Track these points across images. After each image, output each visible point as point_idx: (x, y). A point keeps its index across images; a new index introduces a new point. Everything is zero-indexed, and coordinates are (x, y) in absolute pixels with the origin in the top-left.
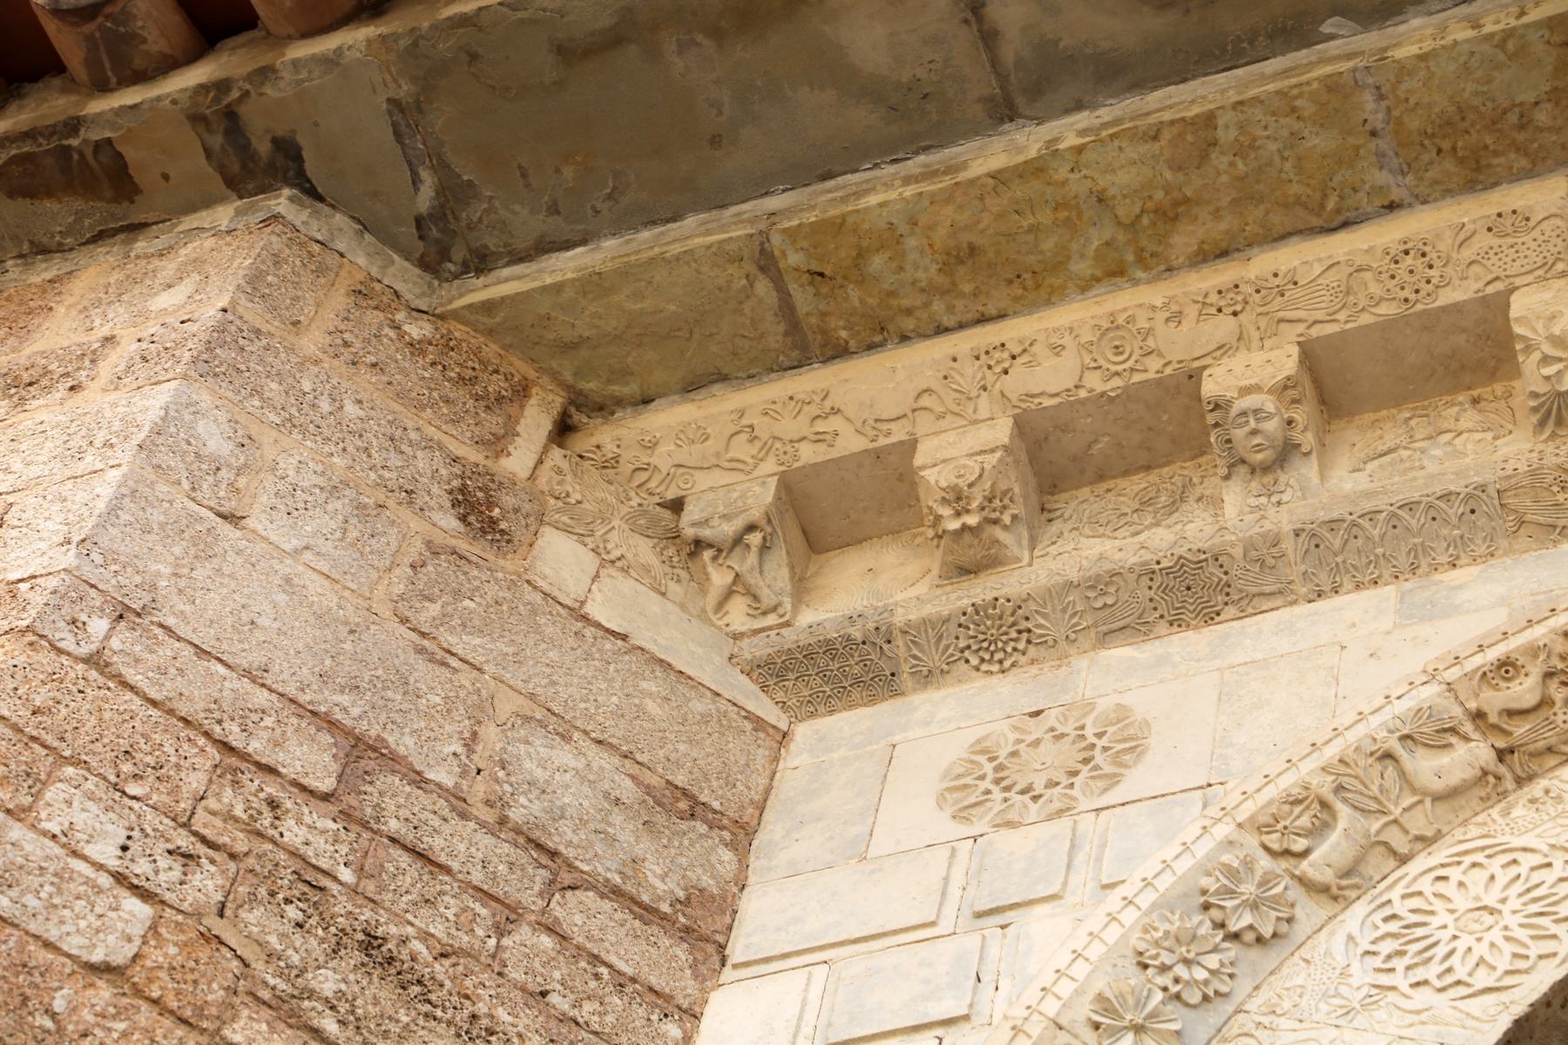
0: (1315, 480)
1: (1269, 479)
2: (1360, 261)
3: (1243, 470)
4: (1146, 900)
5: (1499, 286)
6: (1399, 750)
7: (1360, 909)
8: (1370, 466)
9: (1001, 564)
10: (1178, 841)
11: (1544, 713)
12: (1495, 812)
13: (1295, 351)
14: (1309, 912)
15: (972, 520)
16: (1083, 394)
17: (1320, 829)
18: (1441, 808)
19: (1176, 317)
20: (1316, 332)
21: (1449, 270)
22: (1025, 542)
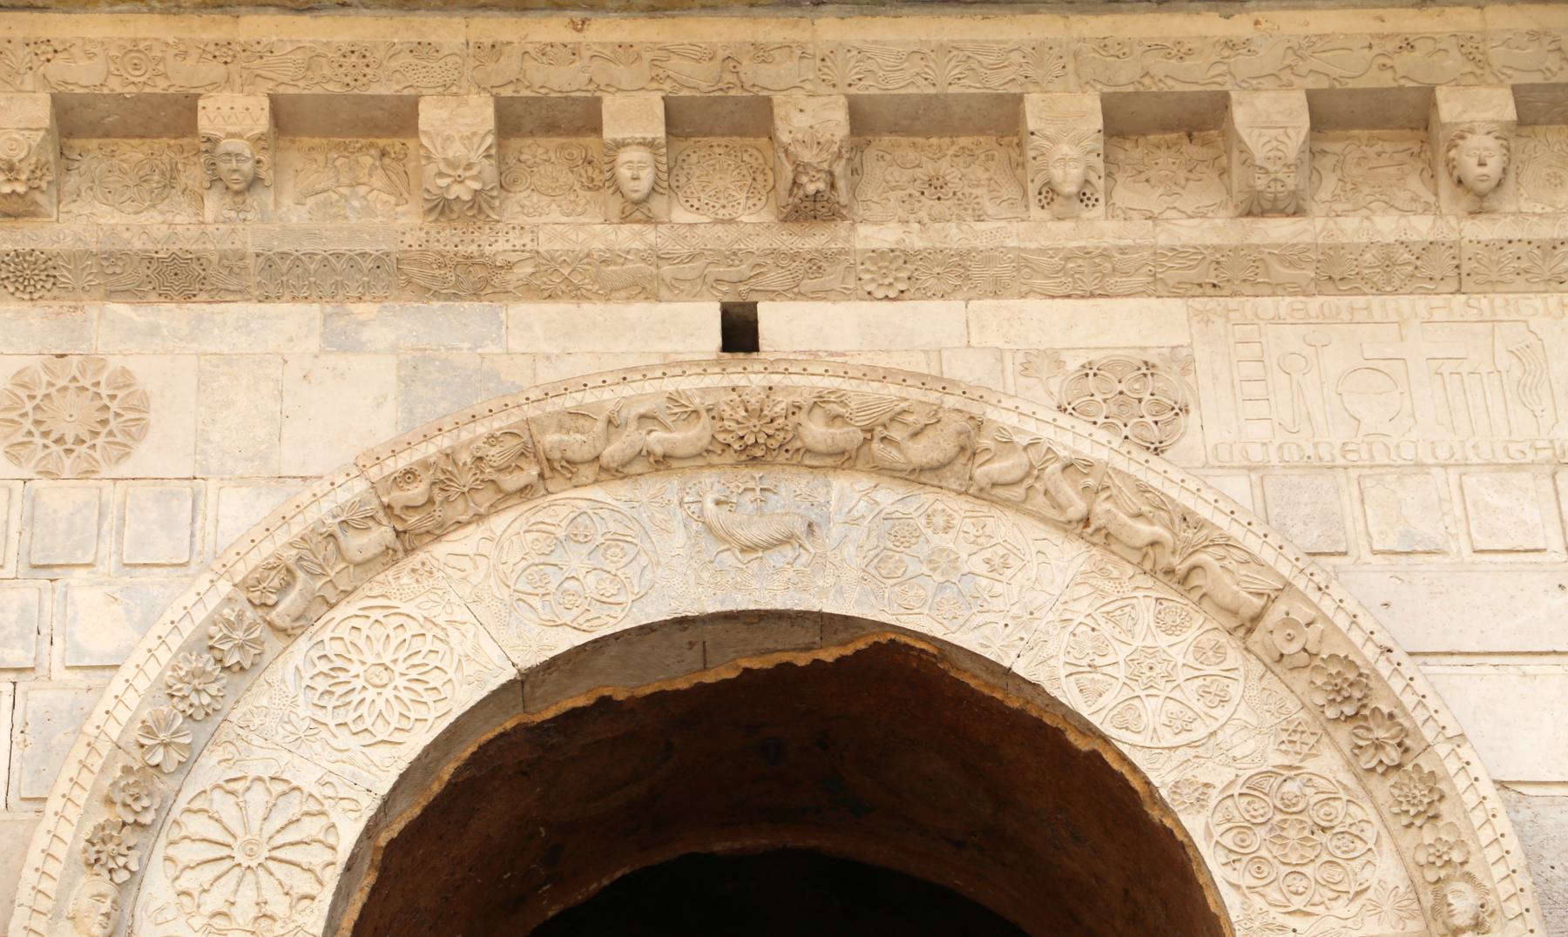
0: (271, 207)
1: (239, 199)
2: (320, 50)
3: (220, 185)
4: (175, 642)
5: (412, 92)
6: (339, 534)
7: (302, 644)
8: (310, 201)
9: (34, 214)
10: (194, 590)
11: (428, 509)
12: (391, 573)
13: (266, 103)
14: (273, 644)
15: (21, 188)
16: (106, 91)
17: (286, 587)
18: (359, 570)
19: (184, 55)
20: (281, 90)
21: (380, 72)
22: (55, 200)
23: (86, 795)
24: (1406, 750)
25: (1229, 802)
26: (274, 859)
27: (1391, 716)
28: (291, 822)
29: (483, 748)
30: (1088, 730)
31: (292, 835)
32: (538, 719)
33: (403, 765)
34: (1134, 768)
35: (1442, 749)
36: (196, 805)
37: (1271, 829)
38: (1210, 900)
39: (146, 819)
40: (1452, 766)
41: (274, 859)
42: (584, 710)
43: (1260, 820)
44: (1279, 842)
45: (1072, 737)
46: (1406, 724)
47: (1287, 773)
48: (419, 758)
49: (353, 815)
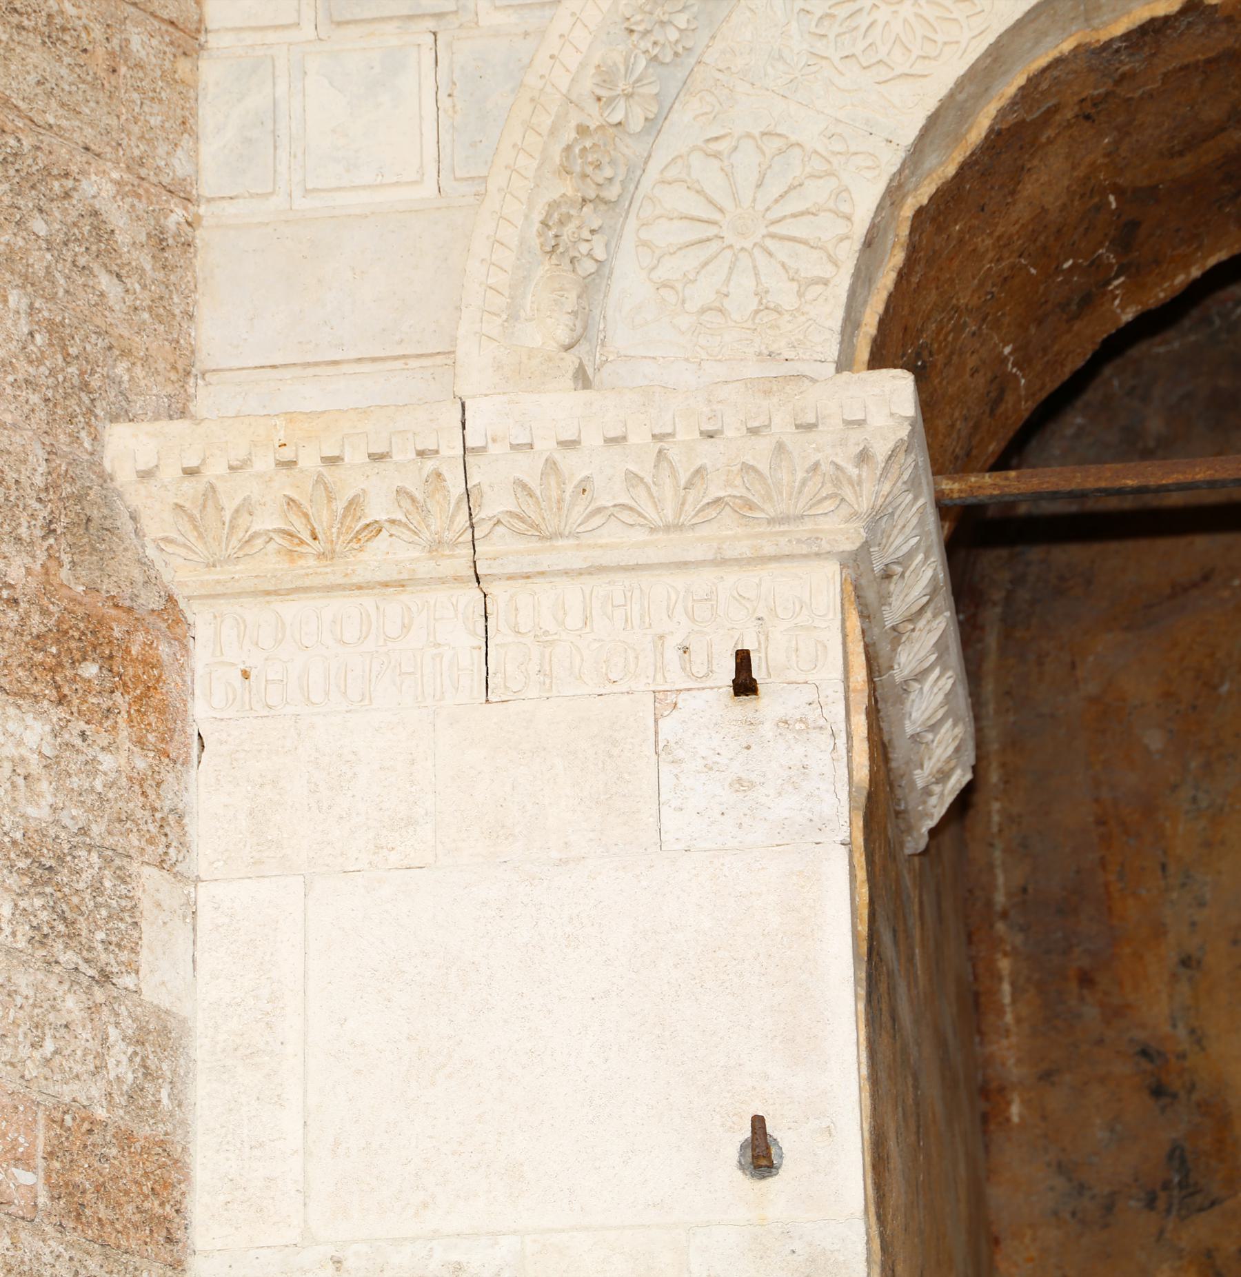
23: (535, 164)
26: (773, 236)
28: (792, 188)
29: (1033, 81)
31: (794, 204)
32: (1104, 36)
33: (931, 105)
36: (672, 173)
39: (612, 193)
41: (773, 236)
42: (1167, 18)
48: (951, 95)
49: (869, 174)
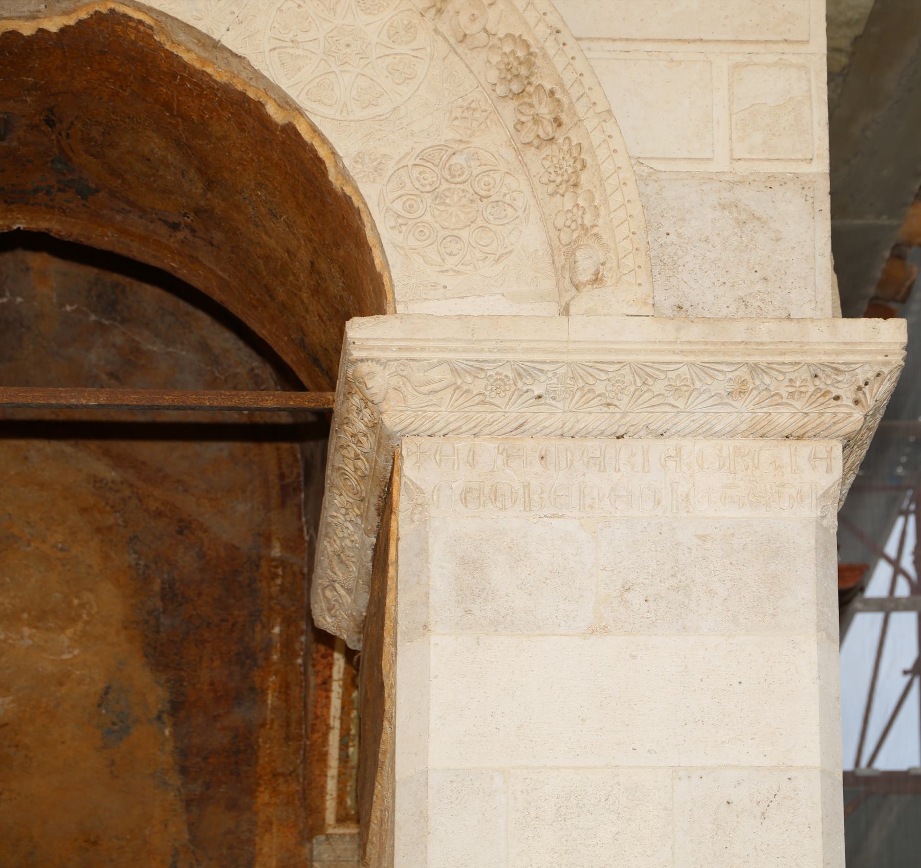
24: (560, 125)
25: (402, 172)
27: (552, 93)
30: (286, 103)
34: (324, 141)
35: (589, 125)
37: (436, 198)
38: (377, 262)
40: (597, 138)
43: (428, 188)
44: (443, 208)
45: (271, 109)
46: (565, 101)
47: (456, 146)
